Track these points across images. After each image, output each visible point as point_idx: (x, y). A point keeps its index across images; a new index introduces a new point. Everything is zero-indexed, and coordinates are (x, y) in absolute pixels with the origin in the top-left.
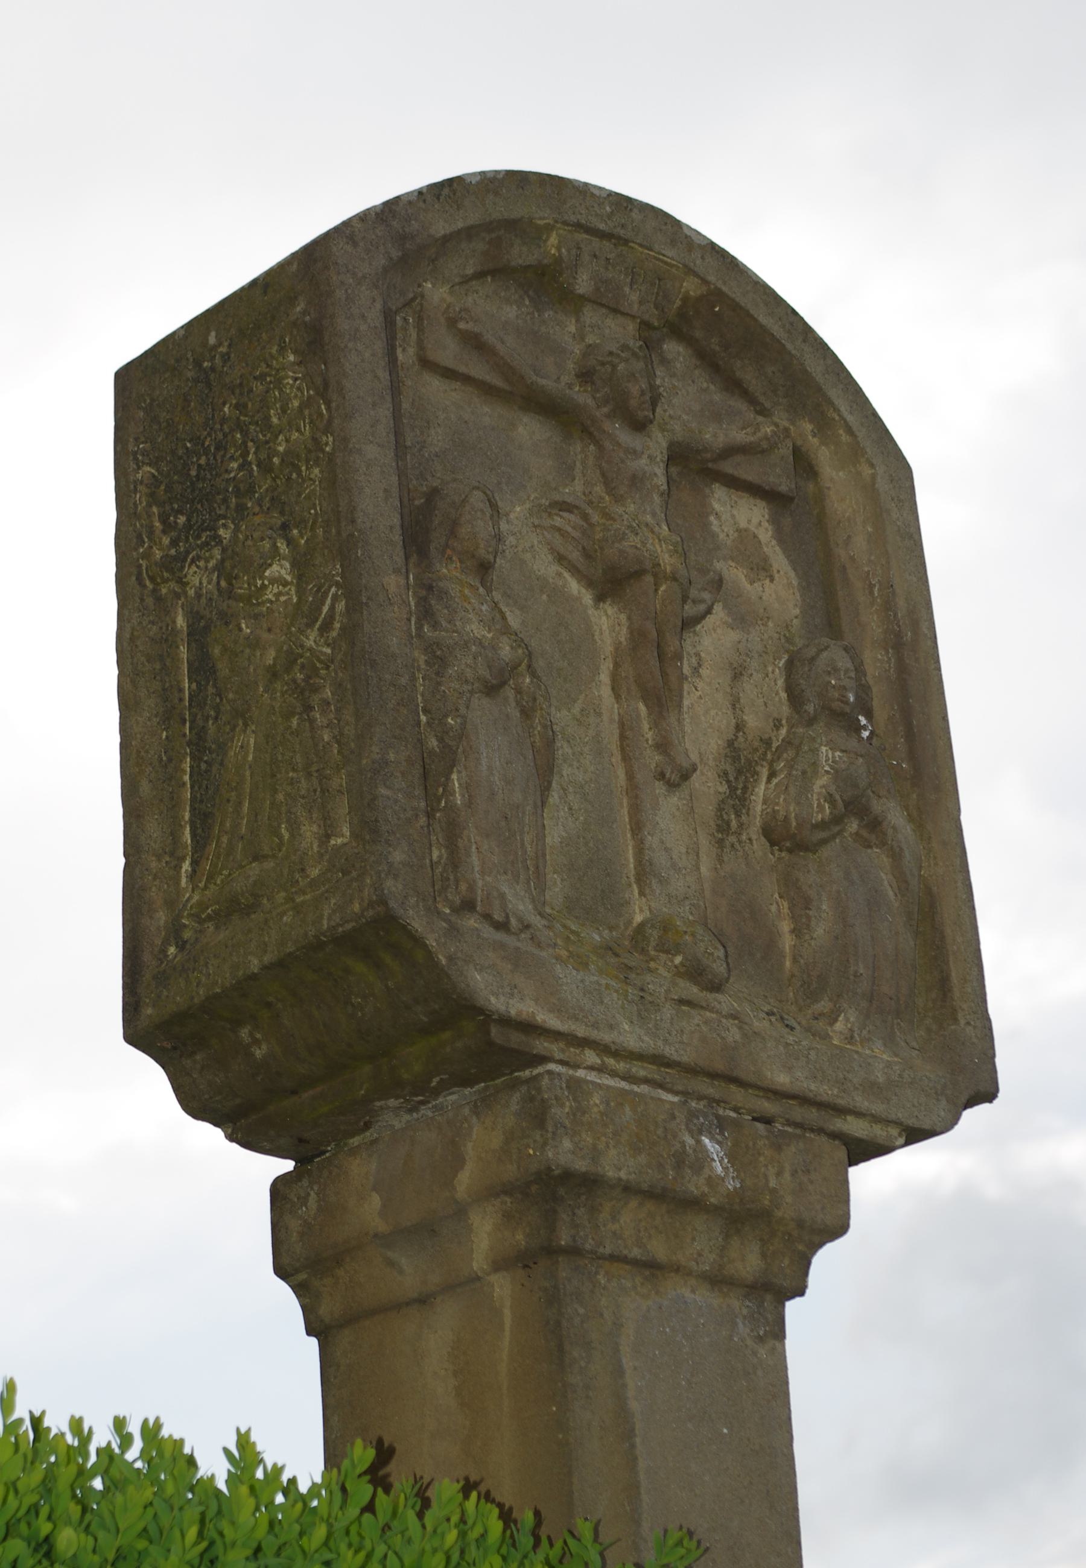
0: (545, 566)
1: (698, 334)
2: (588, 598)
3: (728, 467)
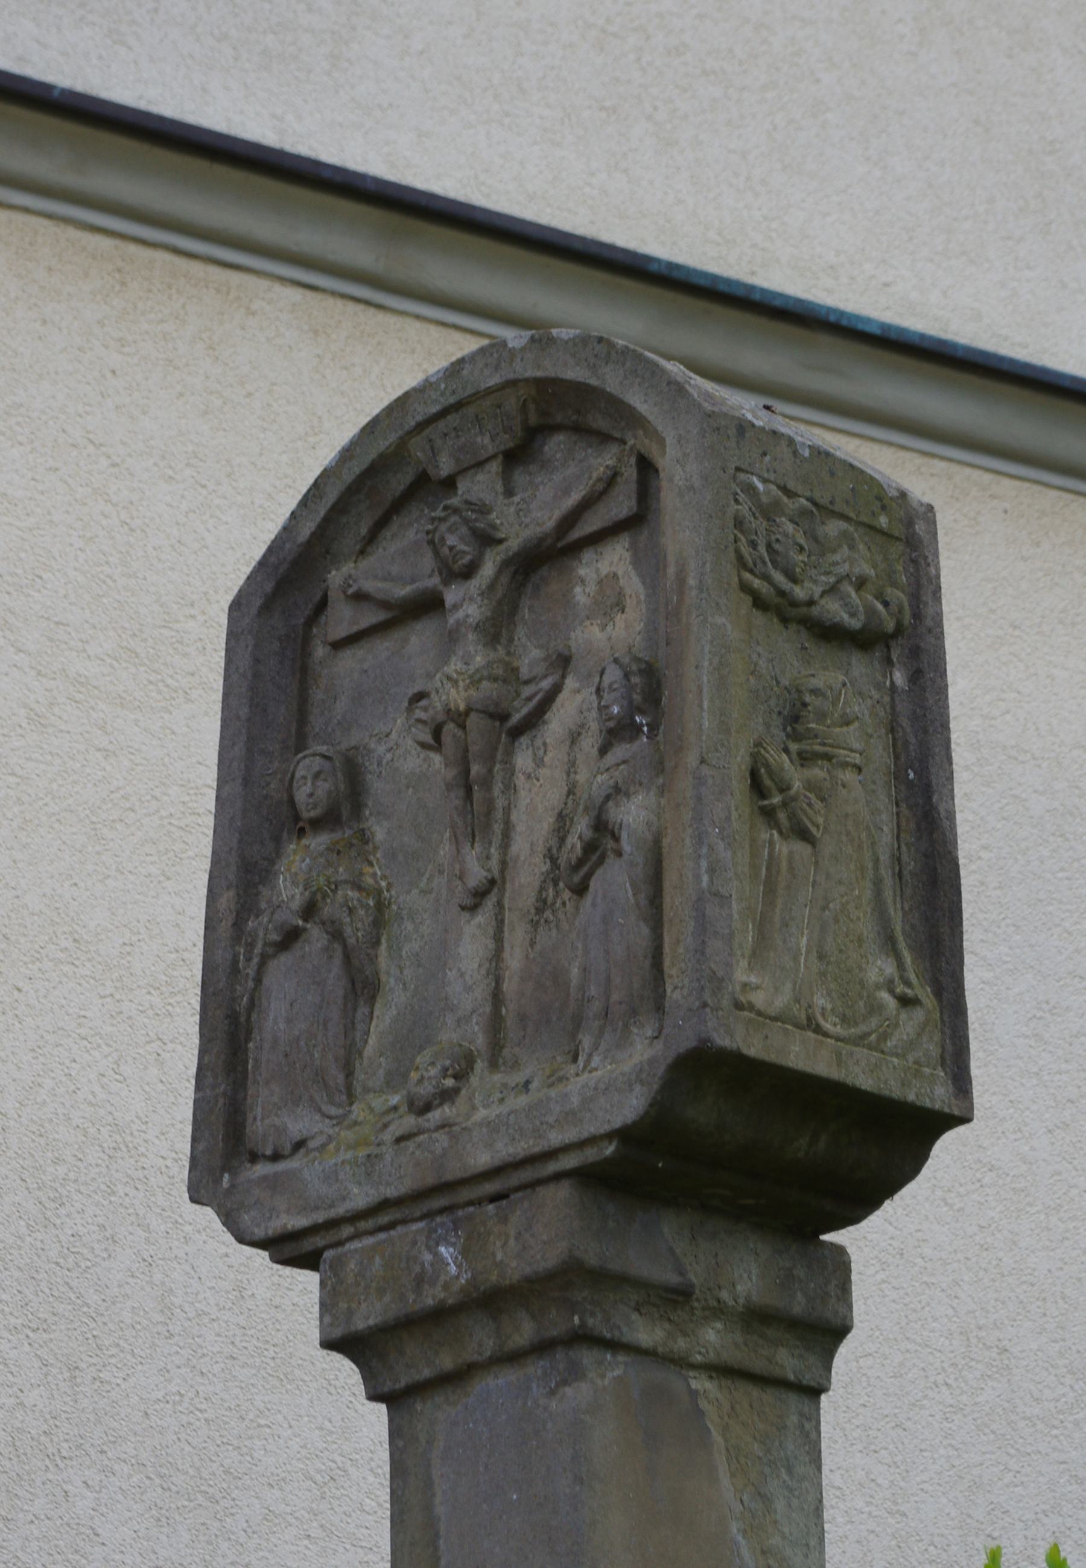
1: (559, 418)
3: (577, 533)
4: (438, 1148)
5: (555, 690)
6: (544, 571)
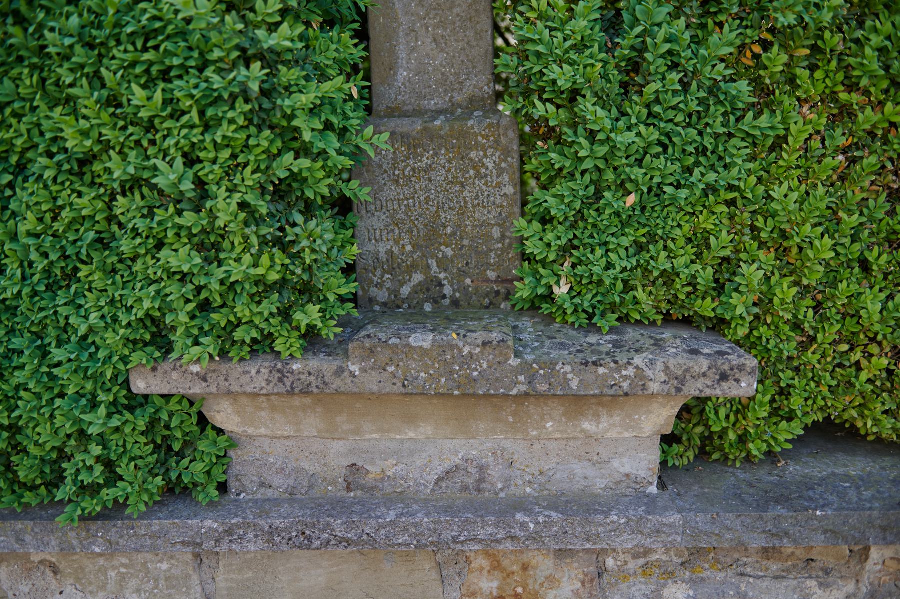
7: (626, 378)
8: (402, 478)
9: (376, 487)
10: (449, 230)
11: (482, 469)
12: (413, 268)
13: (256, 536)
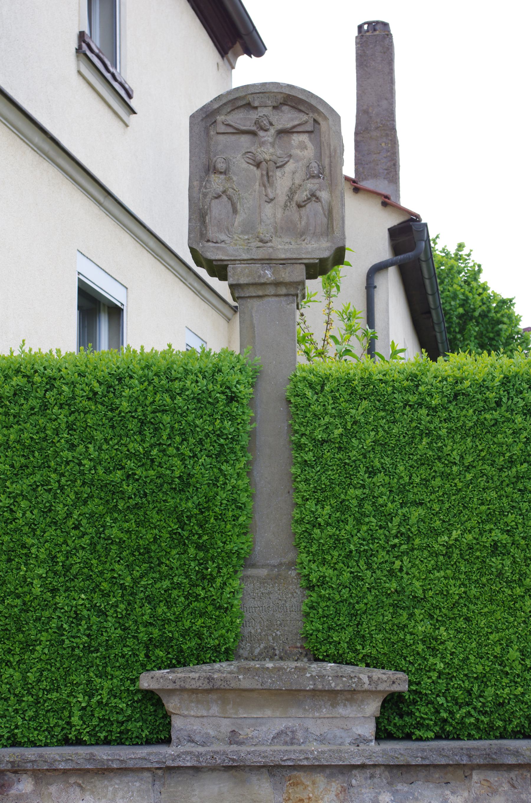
0: (245, 165)
1: (289, 103)
2: (255, 168)
3: (295, 130)
4: (270, 251)
5: (288, 161)
6: (283, 134)
7: (354, 683)
8: (256, 737)
9: (244, 742)
10: (279, 622)
11: (293, 732)
12: (260, 641)
13: (191, 758)
